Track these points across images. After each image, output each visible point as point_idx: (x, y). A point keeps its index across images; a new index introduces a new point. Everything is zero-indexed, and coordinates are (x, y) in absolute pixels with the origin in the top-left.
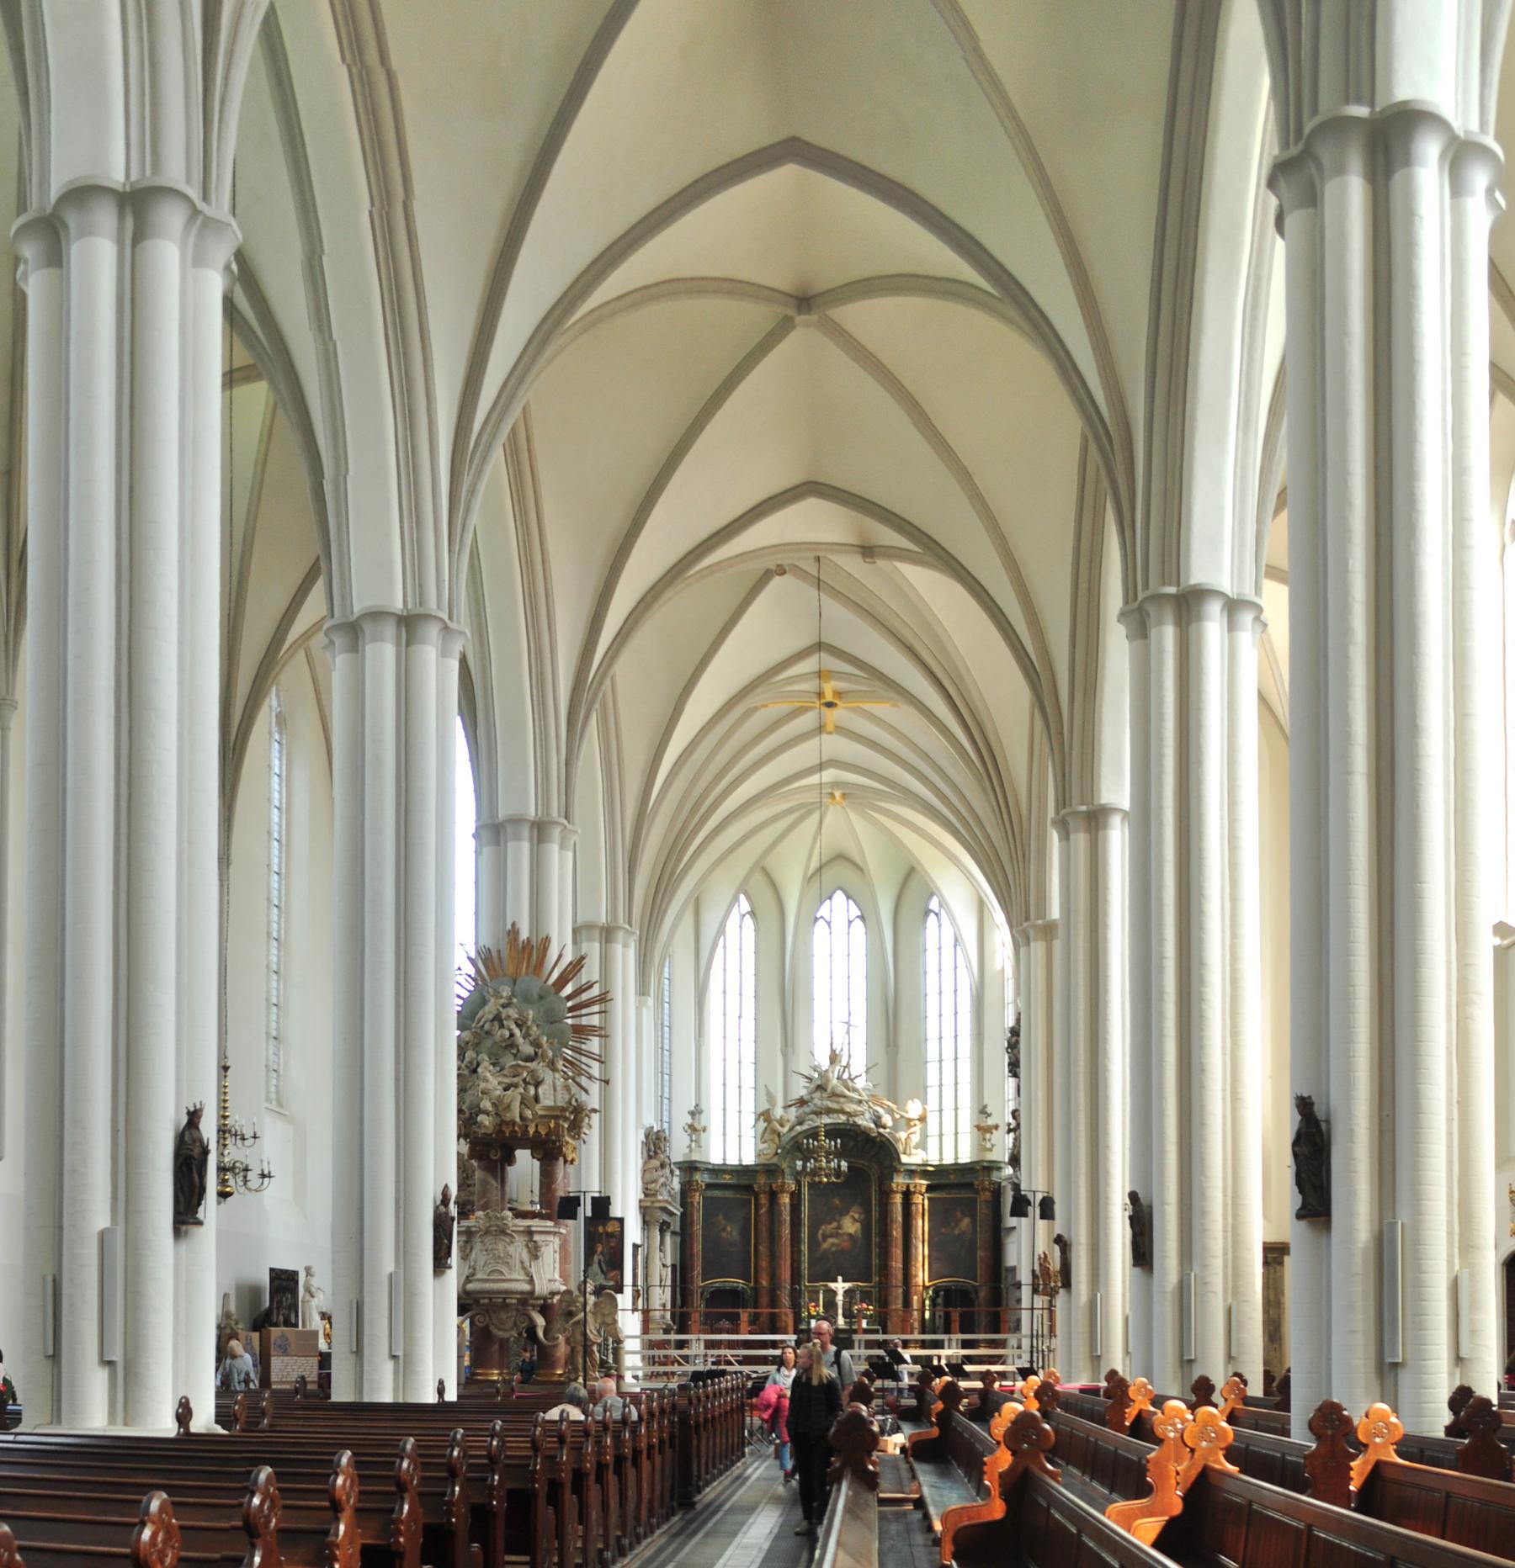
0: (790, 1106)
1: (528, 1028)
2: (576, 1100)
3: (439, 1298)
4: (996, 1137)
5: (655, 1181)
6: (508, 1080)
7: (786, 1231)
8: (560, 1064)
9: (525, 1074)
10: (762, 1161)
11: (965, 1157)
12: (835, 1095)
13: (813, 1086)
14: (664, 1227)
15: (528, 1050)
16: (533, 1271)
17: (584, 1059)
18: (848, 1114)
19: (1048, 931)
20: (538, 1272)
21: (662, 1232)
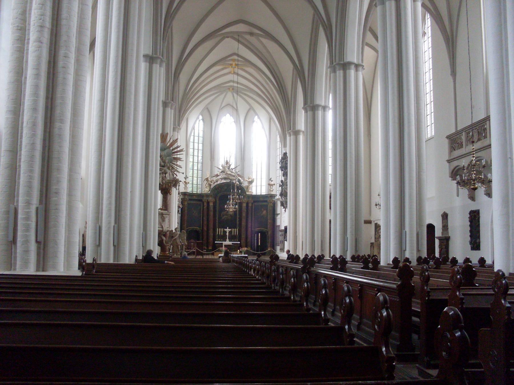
0: (214, 177)
1: (162, 158)
2: (176, 178)
4: (274, 187)
7: (211, 213)
9: (163, 171)
11: (264, 192)
12: (227, 174)
13: (220, 171)
16: (163, 225)
17: (173, 165)
18: (231, 180)
19: (296, 133)
20: (164, 225)
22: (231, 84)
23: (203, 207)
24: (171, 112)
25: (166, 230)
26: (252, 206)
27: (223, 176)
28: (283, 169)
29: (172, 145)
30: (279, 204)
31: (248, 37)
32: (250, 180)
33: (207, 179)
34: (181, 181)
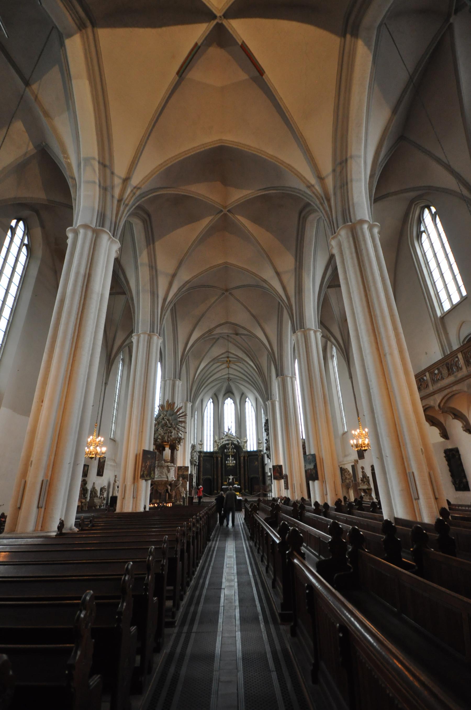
1: (170, 421)
6: (165, 432)
7: (220, 466)
8: (176, 429)
11: (255, 449)
12: (229, 437)
14: (195, 465)
15: (170, 426)
18: (232, 441)
29: (178, 411)
30: (266, 456)
32: (245, 440)
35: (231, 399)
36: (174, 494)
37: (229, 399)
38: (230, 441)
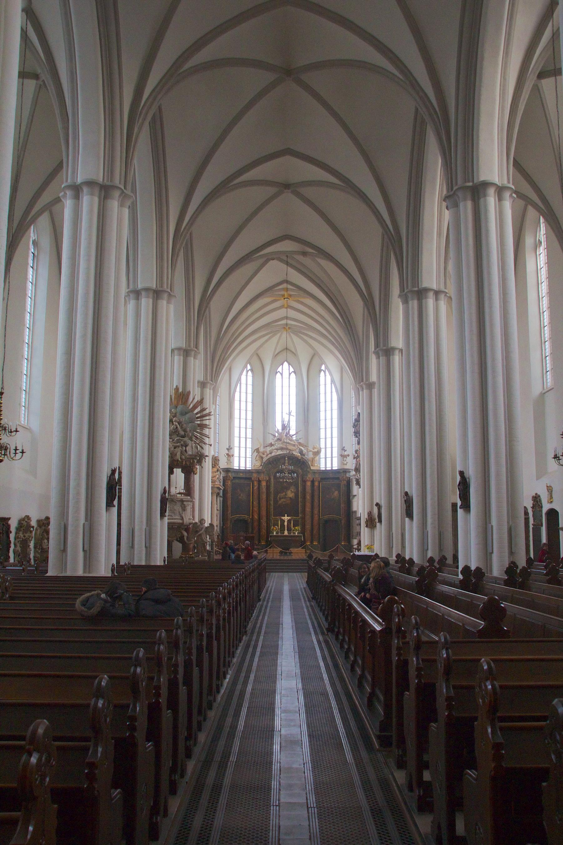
1: (182, 425)
3: (162, 526)
5: (215, 476)
7: (264, 496)
8: (194, 439)
10: (256, 468)
11: (335, 467)
12: (284, 442)
14: (218, 494)
15: (182, 433)
16: (183, 515)
18: (290, 450)
20: (185, 517)
21: (217, 496)
22: (284, 322)
23: (253, 488)
24: (194, 361)
25: (188, 523)
26: (319, 486)
27: (278, 446)
28: (358, 435)
29: (195, 407)
30: (355, 482)
31: (300, 258)
32: (316, 450)
33: (257, 450)
34: (207, 456)
35: (289, 364)
36: (191, 546)
37: (286, 364)
38: (288, 451)
